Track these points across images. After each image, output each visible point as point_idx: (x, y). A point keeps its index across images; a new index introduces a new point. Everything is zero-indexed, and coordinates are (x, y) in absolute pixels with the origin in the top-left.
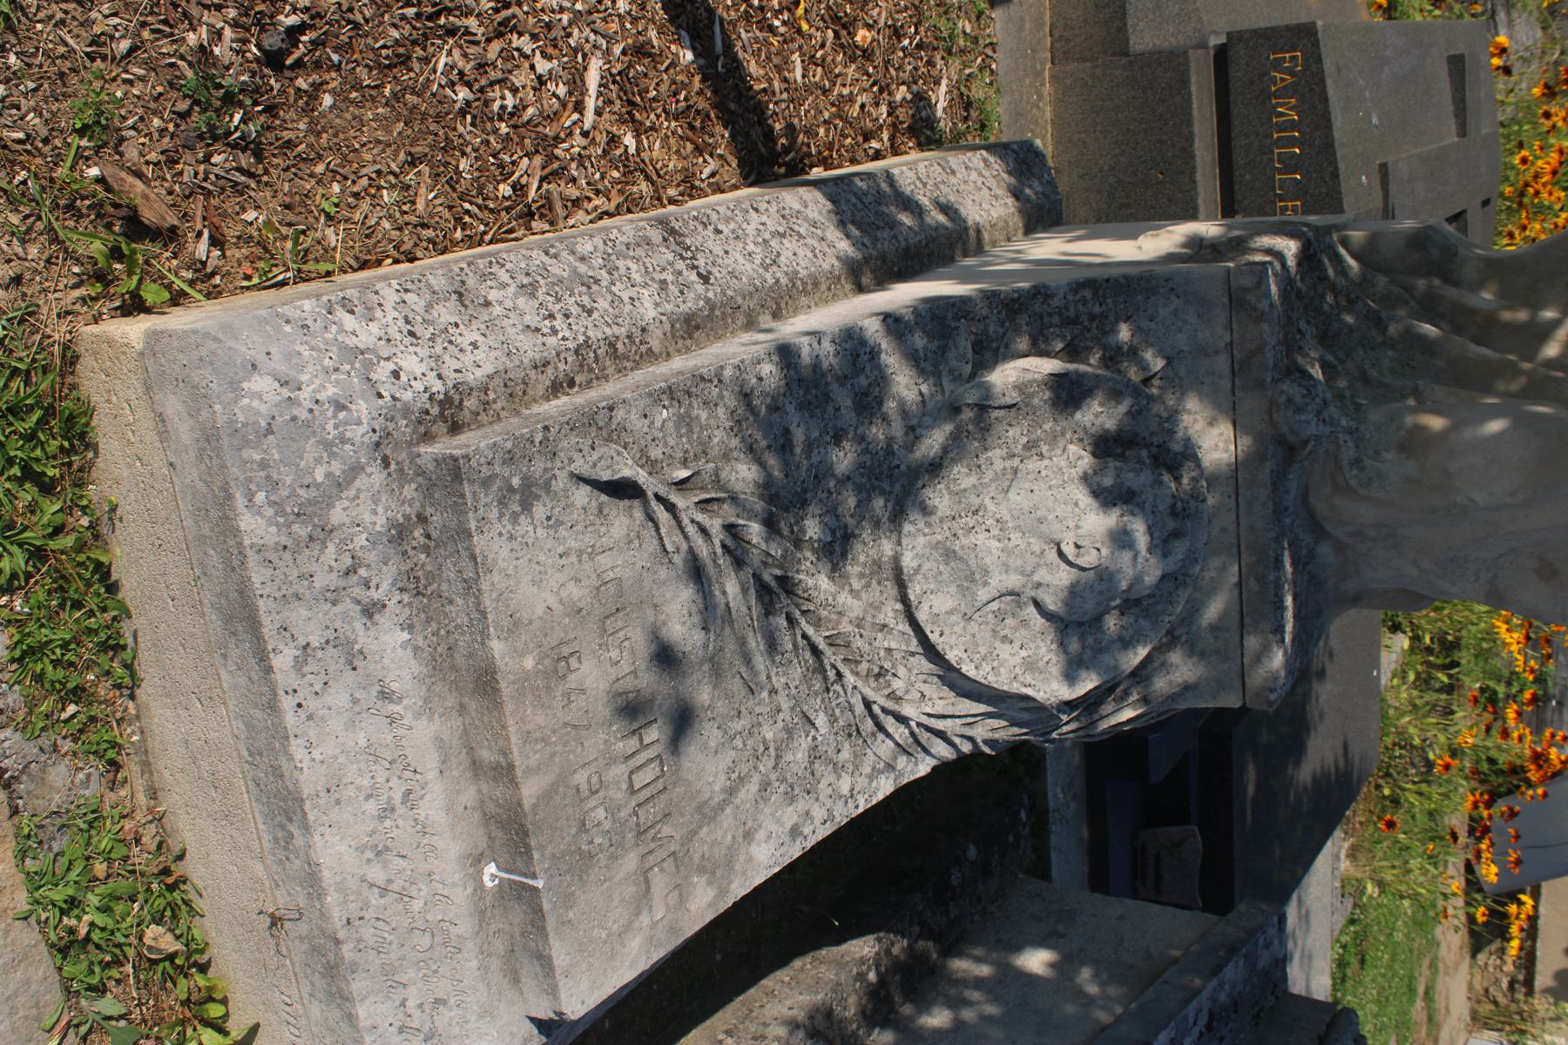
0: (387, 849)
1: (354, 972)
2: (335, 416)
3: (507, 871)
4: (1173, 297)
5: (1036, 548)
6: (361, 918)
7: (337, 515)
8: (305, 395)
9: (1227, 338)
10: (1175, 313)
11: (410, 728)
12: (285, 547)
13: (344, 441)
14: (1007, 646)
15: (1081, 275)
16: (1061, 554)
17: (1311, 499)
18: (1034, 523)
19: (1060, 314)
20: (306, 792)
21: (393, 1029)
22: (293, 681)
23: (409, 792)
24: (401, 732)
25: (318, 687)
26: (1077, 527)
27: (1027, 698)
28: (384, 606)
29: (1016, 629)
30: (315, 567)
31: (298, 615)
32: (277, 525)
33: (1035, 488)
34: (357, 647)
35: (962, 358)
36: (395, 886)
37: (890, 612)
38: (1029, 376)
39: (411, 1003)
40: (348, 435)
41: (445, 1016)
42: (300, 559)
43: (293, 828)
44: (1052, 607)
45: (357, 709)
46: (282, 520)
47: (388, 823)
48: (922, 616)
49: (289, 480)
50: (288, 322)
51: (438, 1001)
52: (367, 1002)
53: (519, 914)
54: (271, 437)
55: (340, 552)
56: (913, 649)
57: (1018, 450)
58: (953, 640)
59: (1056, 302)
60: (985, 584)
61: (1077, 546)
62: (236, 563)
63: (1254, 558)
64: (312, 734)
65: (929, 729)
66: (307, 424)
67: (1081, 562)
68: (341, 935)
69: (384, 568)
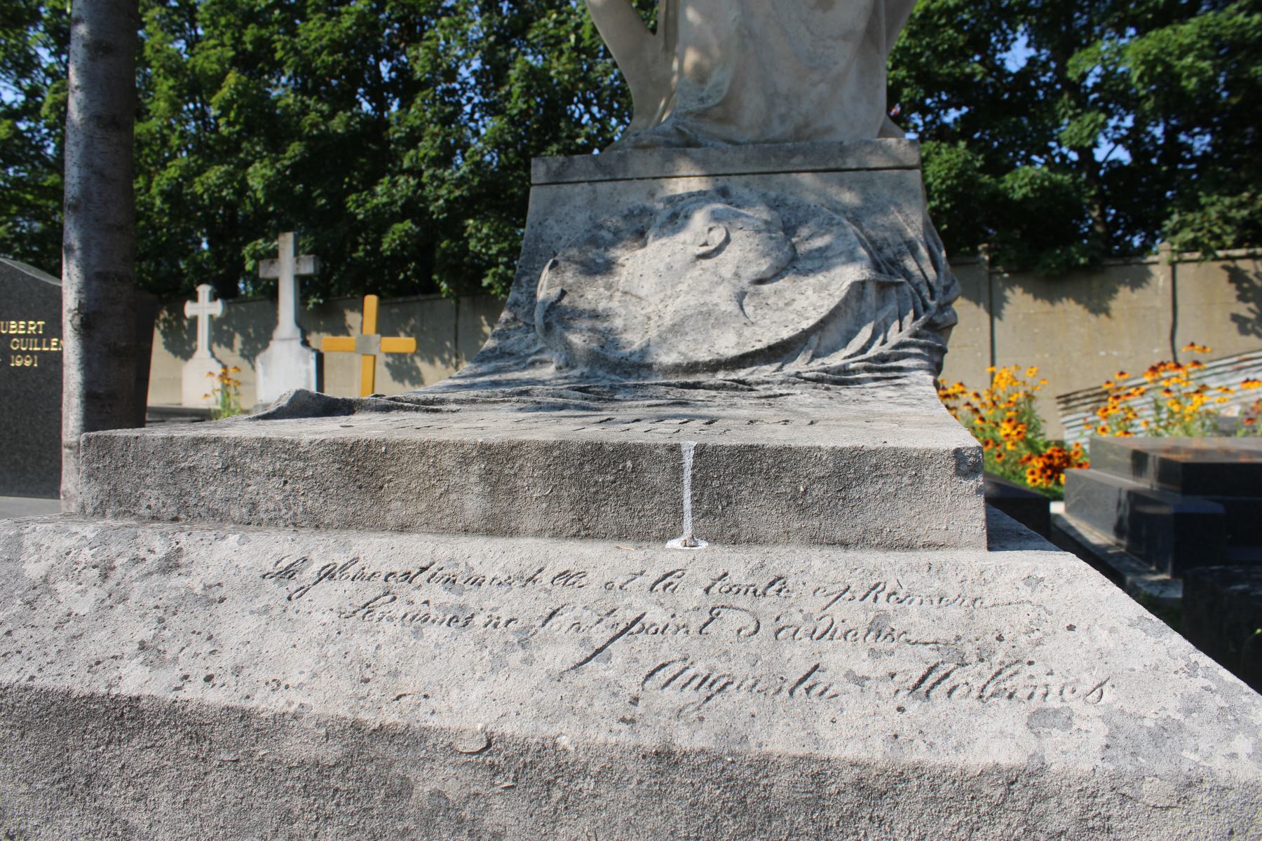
0: (525, 630)
1: (744, 739)
3: (678, 513)
6: (635, 701)
7: (33, 569)
11: (355, 560)
12: (9, 633)
17: (742, 140)
18: (671, 275)
20: (343, 711)
21: (914, 707)
22: (171, 675)
23: (450, 581)
24: (352, 571)
25: (208, 647)
31: (98, 643)
34: (198, 590)
36: (599, 636)
39: (863, 667)
41: (913, 619)
42: (37, 621)
43: (426, 785)
44: (764, 268)
45: (276, 611)
47: (480, 620)
48: (732, 352)
51: (878, 628)
52: (824, 731)
53: (756, 510)
57: (608, 293)
60: (716, 305)
61: (706, 244)
63: (773, 160)
64: (263, 675)
68: (650, 741)
69: (138, 540)
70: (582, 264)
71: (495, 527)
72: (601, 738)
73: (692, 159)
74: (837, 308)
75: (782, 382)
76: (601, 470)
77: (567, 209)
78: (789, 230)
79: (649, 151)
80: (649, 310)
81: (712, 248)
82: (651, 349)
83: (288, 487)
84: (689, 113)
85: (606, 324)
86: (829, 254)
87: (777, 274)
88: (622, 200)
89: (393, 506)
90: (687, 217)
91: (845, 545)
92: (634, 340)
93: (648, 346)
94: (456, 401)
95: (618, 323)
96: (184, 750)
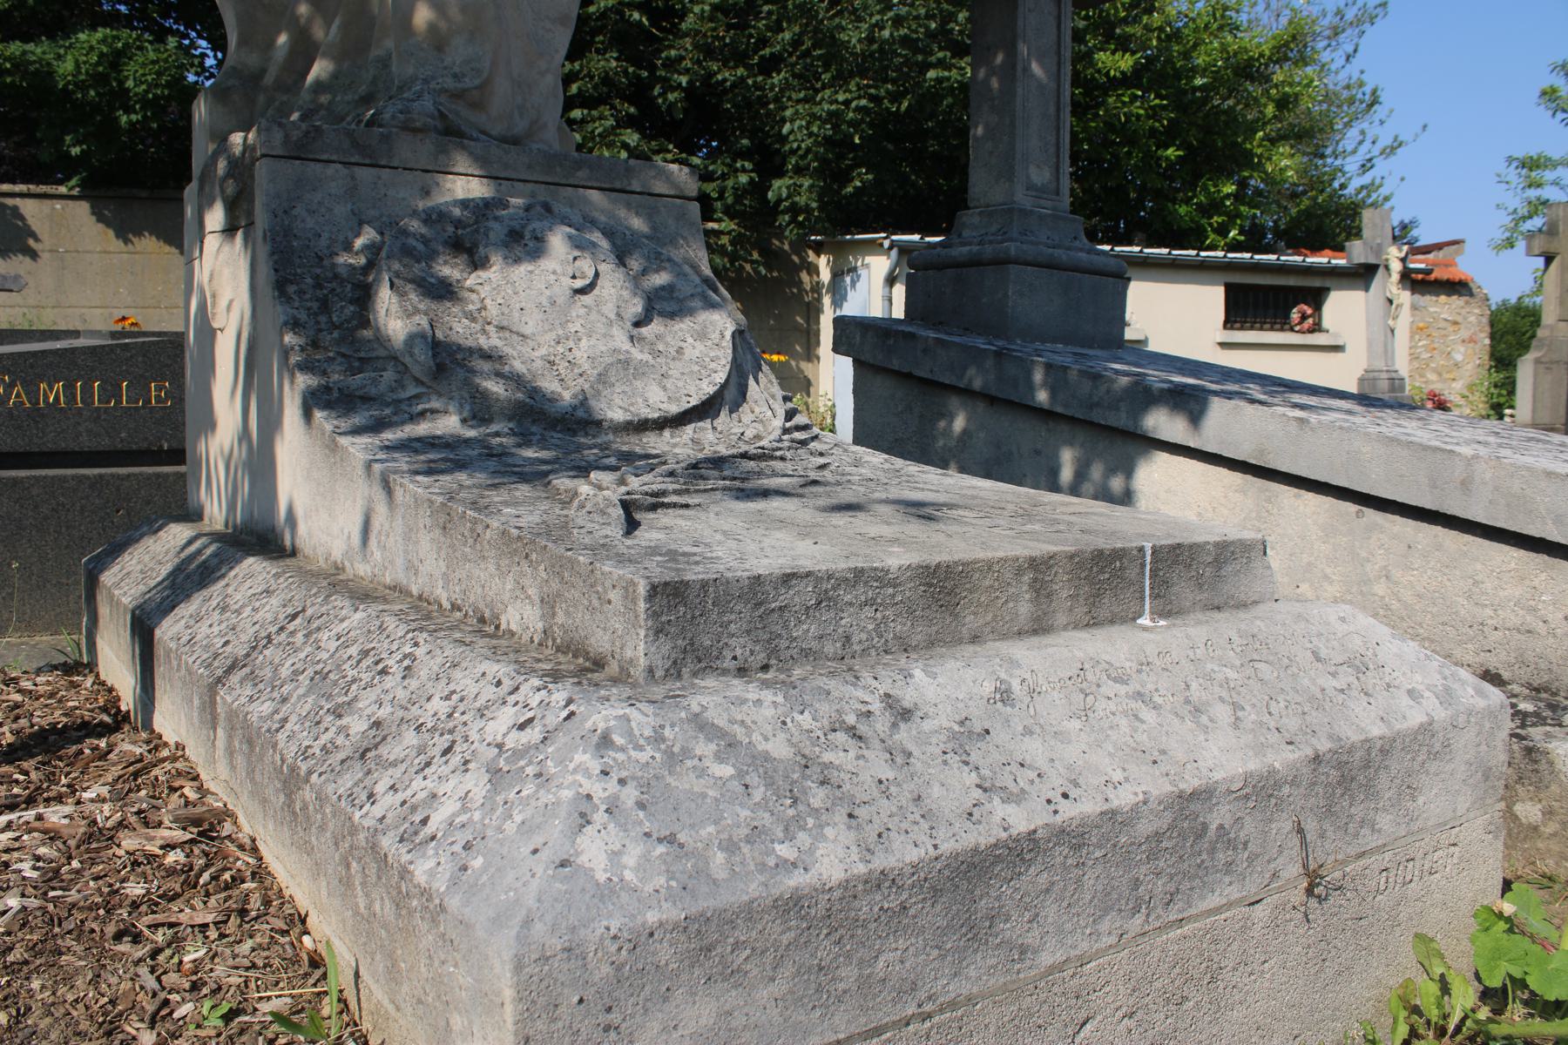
0: (1187, 701)
2: (623, 749)
3: (1142, 599)
4: (294, 212)
5: (582, 311)
8: (600, 790)
10: (312, 212)
13: (658, 738)
15: (267, 291)
16: (582, 291)
17: (493, 133)
19: (316, 314)
25: (1033, 775)
26: (554, 272)
28: (887, 695)
29: (667, 344)
30: (866, 777)
32: (821, 827)
33: (518, 306)
35: (375, 382)
38: (394, 308)
40: (648, 732)
46: (810, 822)
47: (1157, 699)
48: (674, 409)
49: (745, 813)
50: (464, 868)
53: (1183, 591)
54: (682, 837)
55: (831, 747)
59: (303, 316)
61: (574, 277)
62: (893, 903)
66: (646, 787)
67: (591, 273)
68: (1310, 752)
69: (835, 694)
71: (1039, 627)
72: (1291, 756)
73: (471, 154)
74: (735, 359)
75: (789, 448)
76: (1102, 571)
79: (420, 136)
80: (543, 351)
81: (588, 282)
82: (592, 403)
83: (879, 615)
84: (444, 91)
85: (507, 368)
89: (967, 620)
91: (1218, 608)
92: (562, 390)
94: (676, 492)
95: (519, 366)
96: (1070, 861)
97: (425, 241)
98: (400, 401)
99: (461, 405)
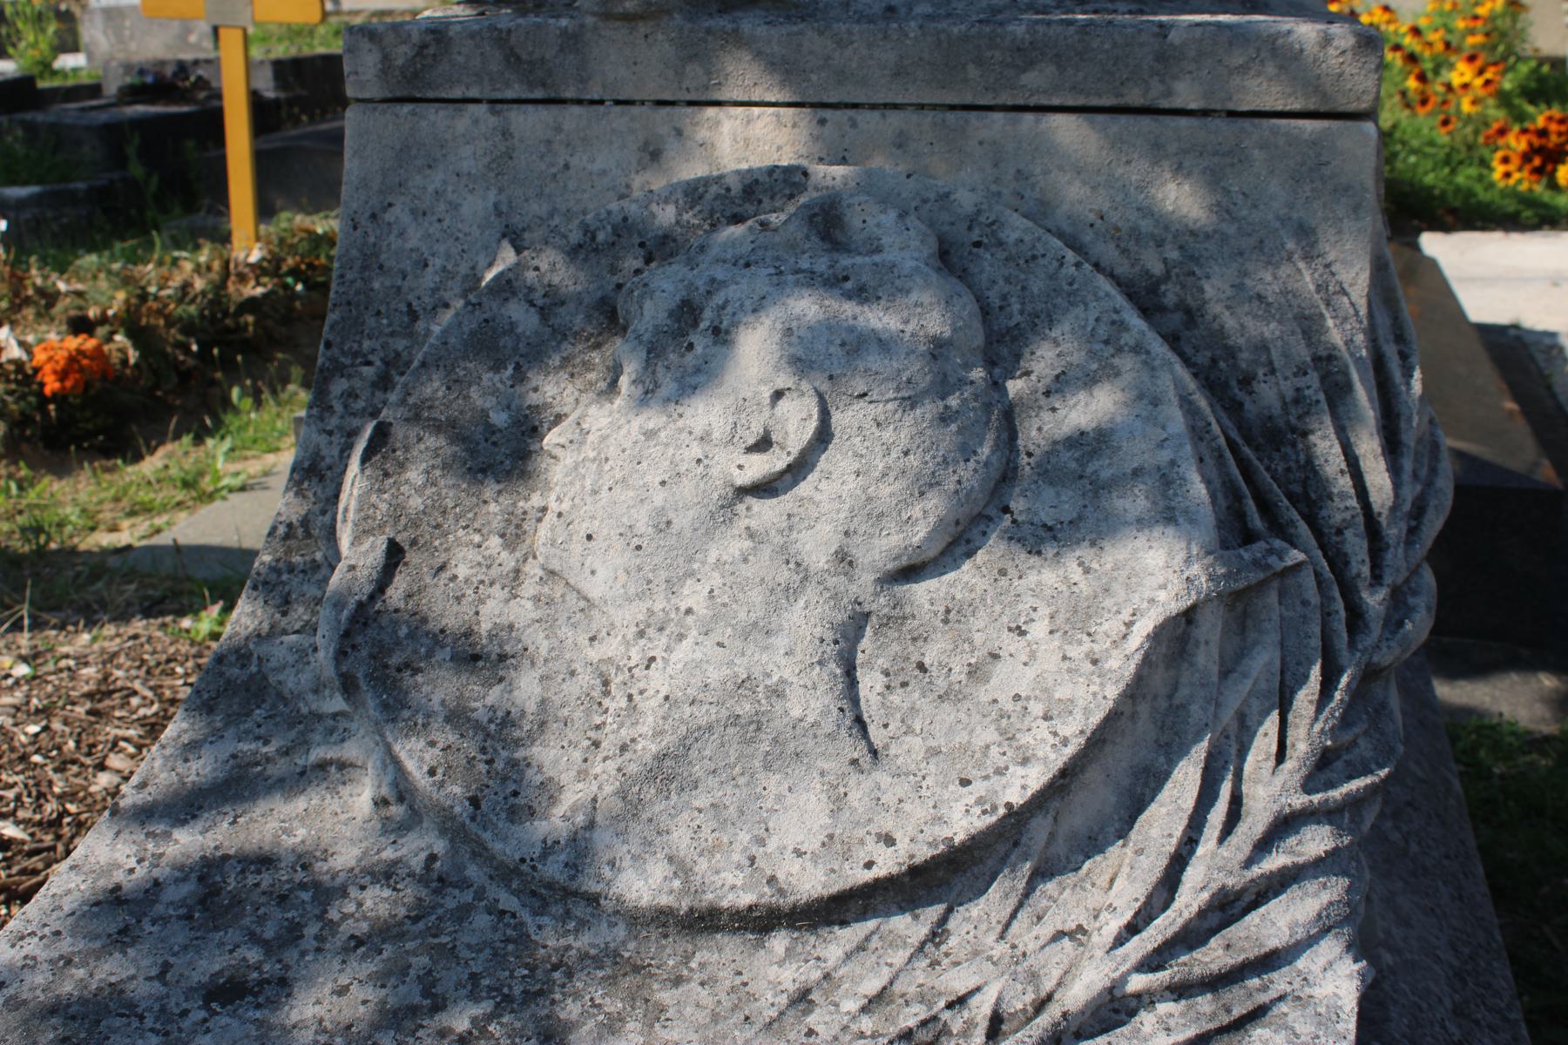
4: (389, 216)
9: (483, 108)
10: (419, 214)
14: (1001, 671)
16: (766, 488)
18: (665, 549)
27: (1175, 637)
33: (583, 528)
37: (777, 966)
38: (353, 505)
44: (920, 533)
56: (923, 931)
57: (508, 560)
58: (918, 812)
60: (777, 692)
61: (763, 444)
63: (973, 72)
65: (1191, 937)
70: (450, 428)
74: (1112, 718)
77: (436, 179)
78: (1003, 346)
79: (642, 28)
80: (610, 648)
82: (602, 837)
85: (494, 695)
86: (1104, 468)
87: (956, 544)
88: (574, 161)
90: (721, 336)
93: (591, 825)
97: (549, 304)
98: (318, 717)
99: (385, 766)
